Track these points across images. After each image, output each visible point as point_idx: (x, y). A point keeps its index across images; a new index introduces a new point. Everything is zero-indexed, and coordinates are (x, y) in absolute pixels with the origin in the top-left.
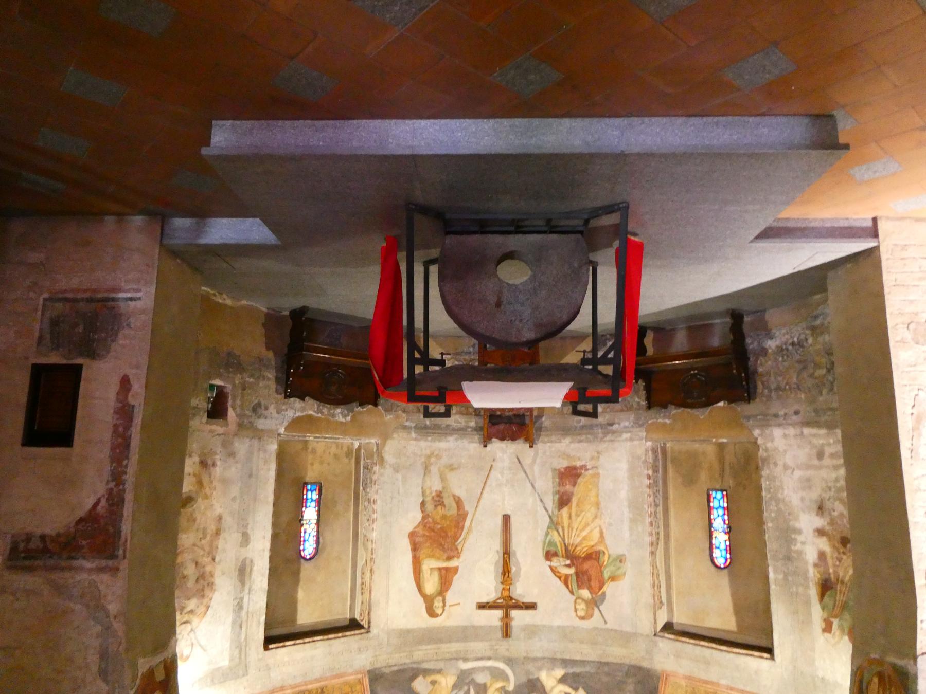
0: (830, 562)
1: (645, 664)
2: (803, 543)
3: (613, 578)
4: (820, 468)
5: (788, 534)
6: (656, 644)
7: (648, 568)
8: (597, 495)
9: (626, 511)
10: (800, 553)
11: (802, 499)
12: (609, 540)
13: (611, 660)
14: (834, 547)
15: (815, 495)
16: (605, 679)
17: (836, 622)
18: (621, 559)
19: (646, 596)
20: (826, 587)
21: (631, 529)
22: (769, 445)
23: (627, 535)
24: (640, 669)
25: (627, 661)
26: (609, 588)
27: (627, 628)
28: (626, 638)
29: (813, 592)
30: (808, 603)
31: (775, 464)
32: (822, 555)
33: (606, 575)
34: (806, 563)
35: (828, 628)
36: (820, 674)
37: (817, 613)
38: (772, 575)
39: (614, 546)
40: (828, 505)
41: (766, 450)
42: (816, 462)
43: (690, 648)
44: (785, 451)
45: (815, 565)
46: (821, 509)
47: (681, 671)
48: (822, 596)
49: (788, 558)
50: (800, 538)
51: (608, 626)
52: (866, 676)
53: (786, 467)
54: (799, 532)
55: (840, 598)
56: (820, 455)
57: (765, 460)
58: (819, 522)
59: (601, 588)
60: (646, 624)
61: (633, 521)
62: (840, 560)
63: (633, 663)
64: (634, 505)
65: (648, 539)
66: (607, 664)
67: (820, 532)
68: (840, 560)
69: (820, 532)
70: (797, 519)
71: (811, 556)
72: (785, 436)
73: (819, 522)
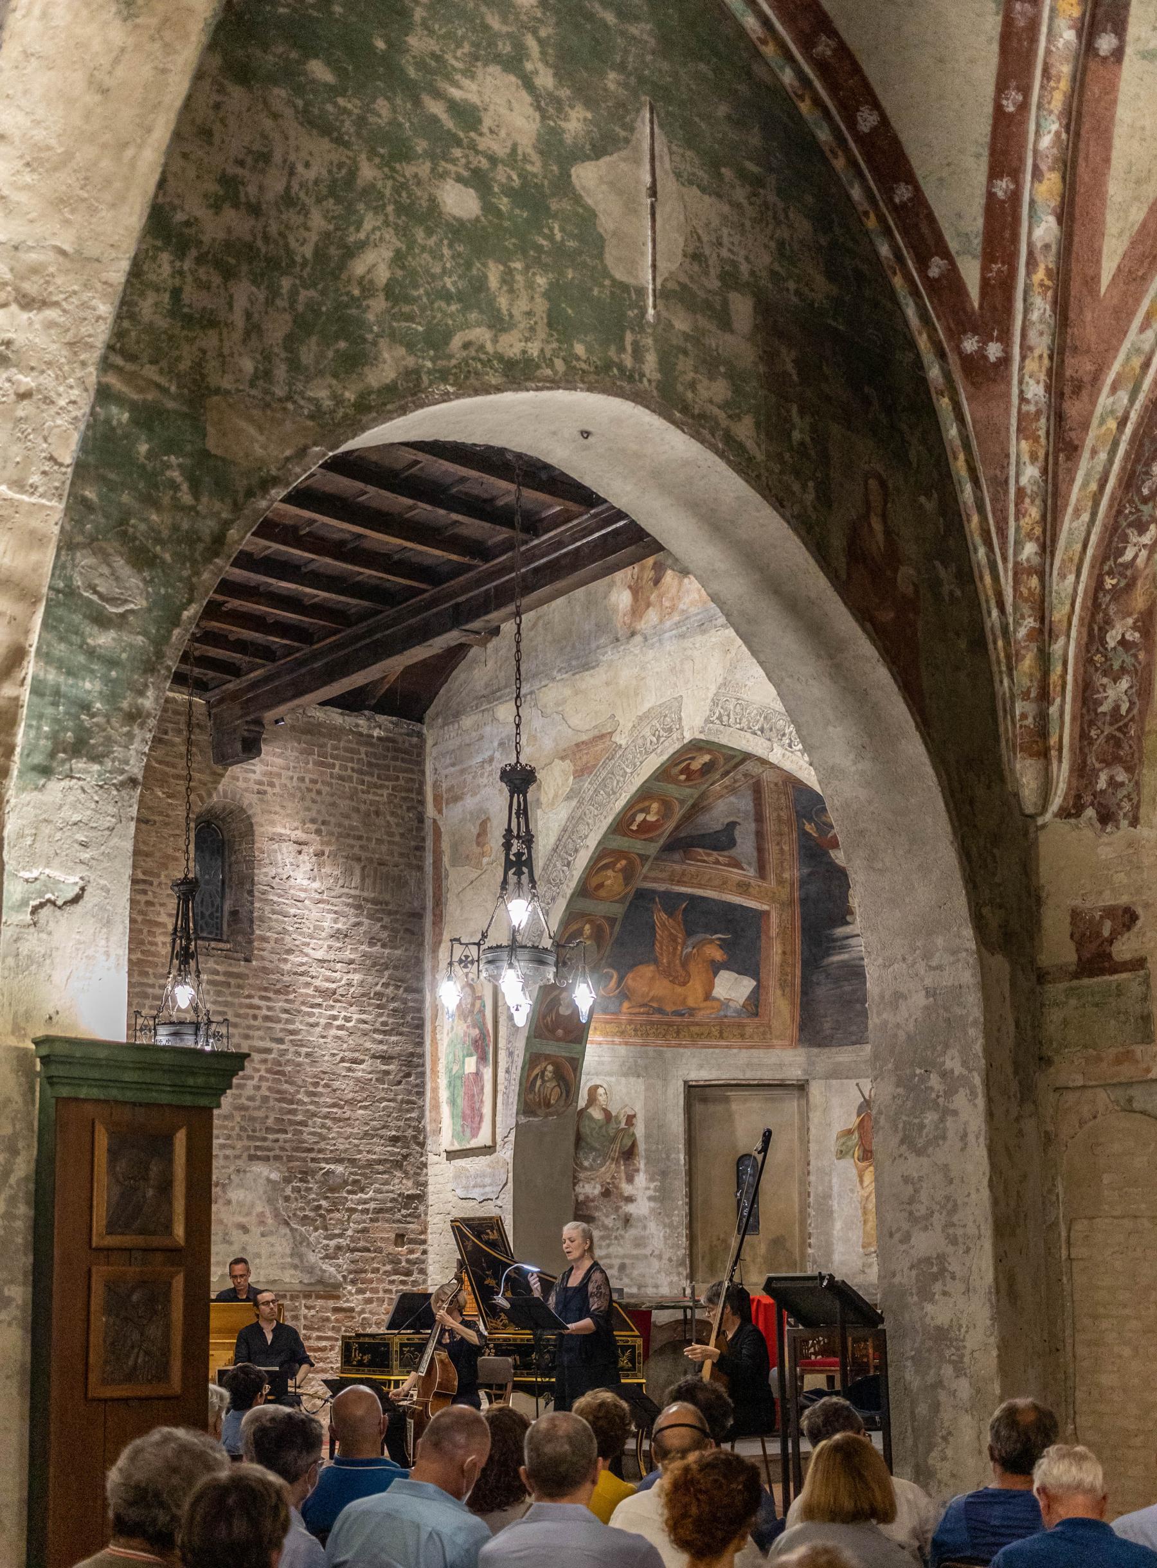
0: (623, 1175)
1: (815, 1050)
2: (648, 1188)
3: (849, 1132)
4: (624, 1256)
5: (662, 1197)
6: (805, 1072)
7: (813, 1147)
8: (865, 1222)
9: (836, 1207)
10: (652, 1180)
11: (645, 1227)
12: (854, 1172)
13: (850, 1048)
14: (617, 1188)
15: (632, 1233)
16: (854, 1028)
17: (623, 1125)
18: (841, 1154)
19: (815, 1117)
20: (629, 1154)
21: (831, 1188)
22: (675, 1279)
23: (835, 1180)
24: (819, 1046)
25: (834, 1050)
26: (853, 1121)
27: (834, 1082)
28: (836, 1073)
29: (641, 1147)
30: (648, 1136)
31: (670, 1260)
32: (630, 1180)
33: (856, 1135)
34: (646, 1172)
35: (630, 1119)
36: (641, 1080)
37: (639, 1130)
38: (682, 1157)
39: (848, 1167)
40: (619, 1224)
41: (679, 1274)
42: (627, 1261)
43: (766, 1075)
44: (659, 1272)
45: (637, 1170)
46: (627, 1220)
47: (777, 1051)
48: (634, 1145)
49: (664, 1174)
50: (651, 1193)
51: (855, 1082)
52: (562, 1103)
53: (660, 1257)
54: (650, 1198)
55: (616, 1147)
56: (622, 1267)
57: (682, 1263)
58: (630, 1208)
59: (862, 1121)
60: (816, 1090)
61: (828, 1196)
62: (613, 1177)
63: (827, 1050)
64: (827, 1214)
65: (812, 1178)
66: (854, 1043)
67: (630, 1199)
68: (613, 1177)
69: (630, 1199)
70: (652, 1210)
71: (641, 1179)
72: (656, 1286)
73: (630, 1208)
